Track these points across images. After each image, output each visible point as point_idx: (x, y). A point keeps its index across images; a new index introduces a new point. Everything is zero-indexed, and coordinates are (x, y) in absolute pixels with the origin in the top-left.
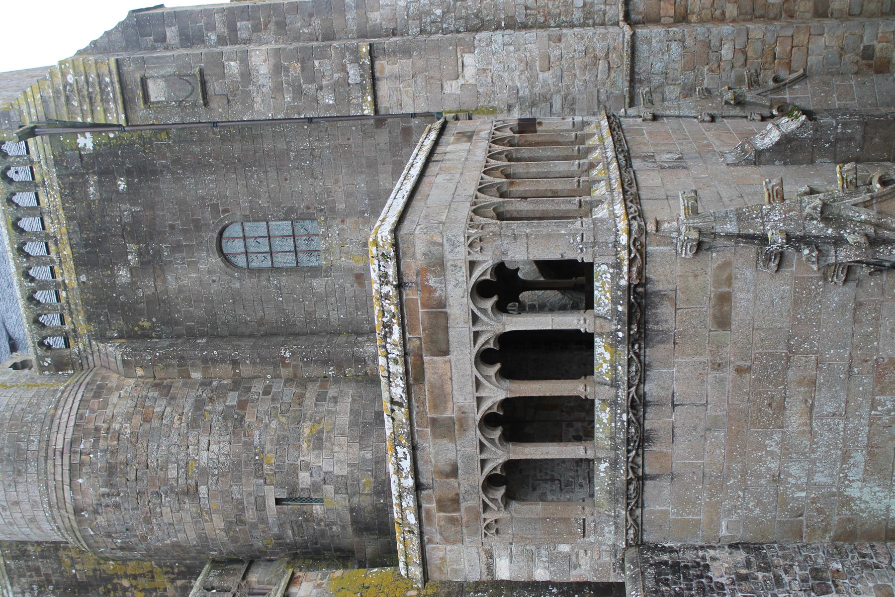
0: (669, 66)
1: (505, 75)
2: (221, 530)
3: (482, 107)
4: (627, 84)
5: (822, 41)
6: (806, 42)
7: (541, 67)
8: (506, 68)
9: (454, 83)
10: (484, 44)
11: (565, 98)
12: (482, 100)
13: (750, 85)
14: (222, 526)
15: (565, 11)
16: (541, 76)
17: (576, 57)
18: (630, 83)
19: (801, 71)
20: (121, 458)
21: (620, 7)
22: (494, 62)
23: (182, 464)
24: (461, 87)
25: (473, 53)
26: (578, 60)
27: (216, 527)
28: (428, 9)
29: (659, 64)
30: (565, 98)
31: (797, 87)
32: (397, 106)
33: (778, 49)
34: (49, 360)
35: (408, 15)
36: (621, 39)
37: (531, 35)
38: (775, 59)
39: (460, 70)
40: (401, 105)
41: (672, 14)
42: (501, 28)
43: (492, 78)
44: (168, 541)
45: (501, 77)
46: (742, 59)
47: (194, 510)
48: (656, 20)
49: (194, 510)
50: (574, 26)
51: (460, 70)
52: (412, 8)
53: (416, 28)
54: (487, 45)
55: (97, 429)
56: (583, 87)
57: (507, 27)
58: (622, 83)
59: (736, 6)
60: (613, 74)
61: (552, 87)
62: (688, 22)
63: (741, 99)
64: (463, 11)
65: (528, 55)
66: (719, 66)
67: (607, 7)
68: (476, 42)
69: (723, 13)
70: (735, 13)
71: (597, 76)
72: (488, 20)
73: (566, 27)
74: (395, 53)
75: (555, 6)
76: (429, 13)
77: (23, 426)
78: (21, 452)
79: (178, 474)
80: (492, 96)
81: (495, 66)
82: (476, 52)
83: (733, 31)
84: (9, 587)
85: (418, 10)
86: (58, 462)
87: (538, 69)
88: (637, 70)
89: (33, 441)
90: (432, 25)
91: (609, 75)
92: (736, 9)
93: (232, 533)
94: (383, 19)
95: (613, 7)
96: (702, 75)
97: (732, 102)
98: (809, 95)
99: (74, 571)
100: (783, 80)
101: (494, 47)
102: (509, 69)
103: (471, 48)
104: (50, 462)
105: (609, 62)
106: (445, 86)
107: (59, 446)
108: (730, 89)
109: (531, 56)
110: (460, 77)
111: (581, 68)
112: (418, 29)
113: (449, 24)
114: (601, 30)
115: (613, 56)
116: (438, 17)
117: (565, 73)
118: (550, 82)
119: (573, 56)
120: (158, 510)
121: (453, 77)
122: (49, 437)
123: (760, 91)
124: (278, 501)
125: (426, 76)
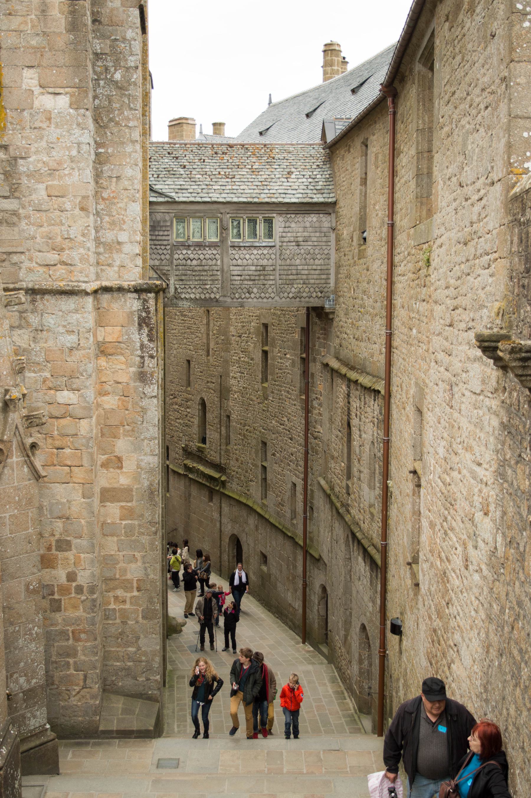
0: (50, 334)
1: (44, 144)
3: (6, 114)
4: (30, 286)
5: (77, 498)
6: (75, 480)
7: (51, 186)
8: (52, 145)
9: (35, 82)
10: (80, 120)
11: (15, 213)
12: (14, 114)
13: (28, 417)
15: (114, 221)
16: (42, 186)
17: (63, 228)
18: (31, 289)
19: (43, 473)
21: (116, 282)
22: (59, 131)
24: (30, 90)
25: (71, 106)
26: (59, 230)
28: (122, 64)
29: (53, 322)
30: (15, 214)
31: (26, 469)
32: (8, 9)
33: (67, 451)
35: (116, 40)
36: (82, 279)
37: (88, 174)
38: (58, 449)
39: (51, 90)
40: (10, 14)
41: (107, 340)
42: (97, 148)
43: (40, 128)
45: (41, 139)
46: (57, 414)
48: (100, 323)
50: (97, 232)
51: (51, 90)
52: (123, 45)
53: (101, 48)
54: (78, 125)
56: (27, 235)
57: (97, 154)
58: (32, 281)
59: (114, 407)
60: (42, 270)
61: (27, 199)
62: (97, 357)
63: (11, 407)
64: (118, 105)
65: (66, 172)
66: (50, 389)
67: (116, 269)
68: (82, 111)
69: (107, 394)
70: (107, 406)
71: (40, 251)
72: (106, 133)
73: (96, 221)
74: (73, 12)
75: (119, 210)
76: (117, 65)
80: (18, 127)
81: (53, 133)
82: (71, 111)
83: (88, 403)
85: (121, 53)
87: (50, 183)
88: (46, 297)
90: (103, 69)
91: (40, 265)
92: (111, 407)
94: (112, 10)
95: (117, 275)
96: (41, 370)
97: (8, 397)
98: (16, 484)
100: (33, 454)
101: (77, 131)
102: (50, 148)
103: (75, 105)
105: (55, 265)
106: (32, 71)
108: (24, 395)
109: (65, 175)
110: (42, 90)
111: (50, 233)
112: (99, 51)
113: (104, 87)
114: (92, 259)
115: (61, 270)
116: (112, 76)
117: (44, 214)
118: (34, 197)
119: (63, 225)
121: (42, 81)
123: (20, 427)
125: (44, 48)
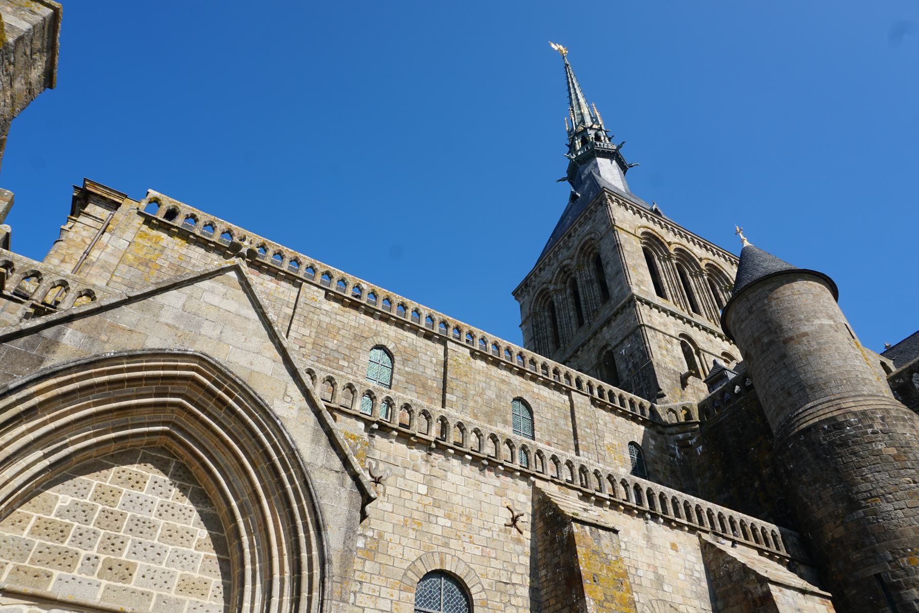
2: (833, 536)
14: (837, 536)
20: (857, 448)
23: (874, 493)
27: (833, 531)
34: (901, 381)
44: (805, 500)
47: (840, 511)
49: (840, 511)
55: (871, 426)
77: (845, 380)
78: (827, 384)
79: (864, 492)
84: (727, 415)
86: (832, 409)
89: (839, 389)
93: (833, 545)
99: (753, 449)
104: (830, 404)
107: (843, 406)
120: (828, 485)
122: (847, 397)
124: (878, 576)
